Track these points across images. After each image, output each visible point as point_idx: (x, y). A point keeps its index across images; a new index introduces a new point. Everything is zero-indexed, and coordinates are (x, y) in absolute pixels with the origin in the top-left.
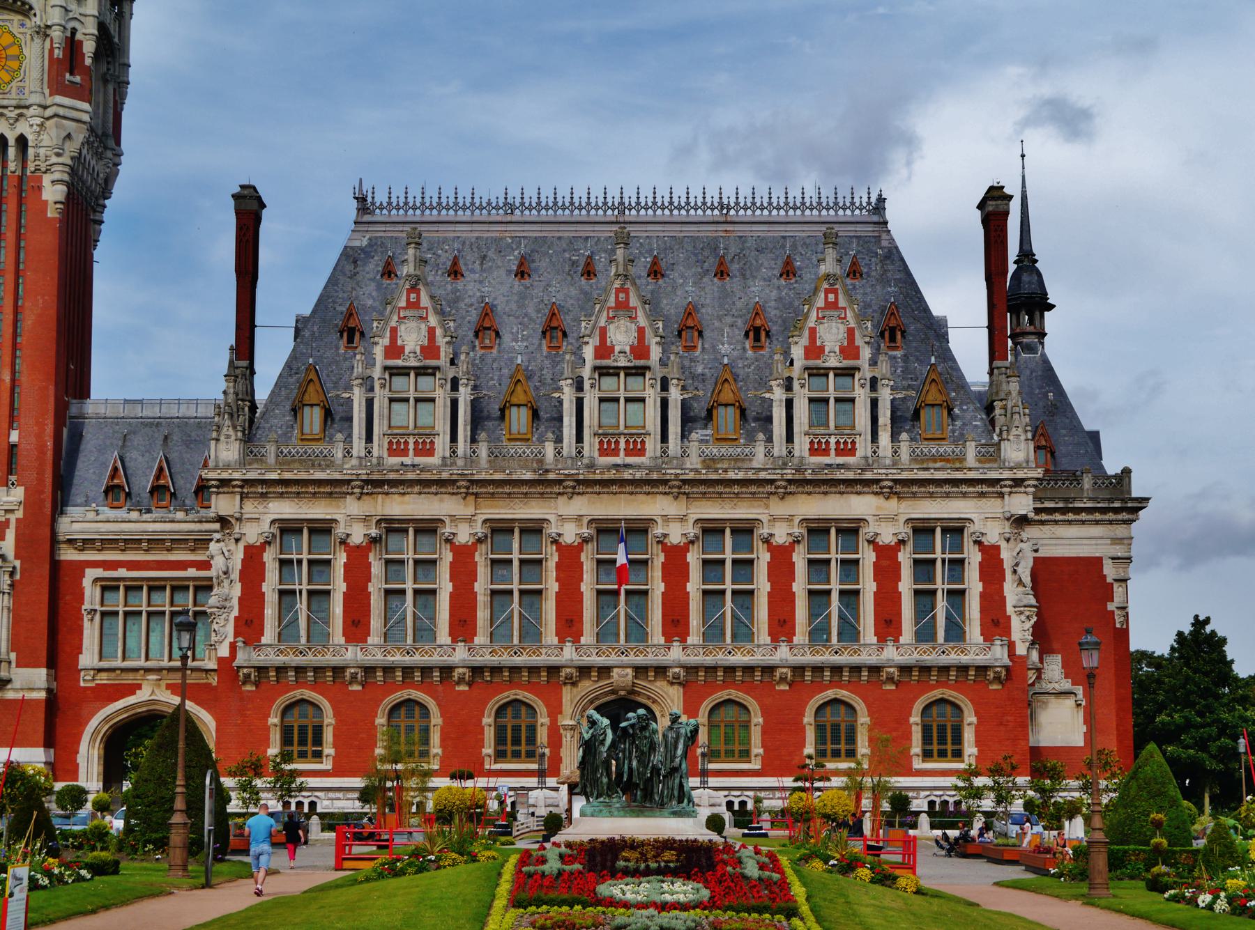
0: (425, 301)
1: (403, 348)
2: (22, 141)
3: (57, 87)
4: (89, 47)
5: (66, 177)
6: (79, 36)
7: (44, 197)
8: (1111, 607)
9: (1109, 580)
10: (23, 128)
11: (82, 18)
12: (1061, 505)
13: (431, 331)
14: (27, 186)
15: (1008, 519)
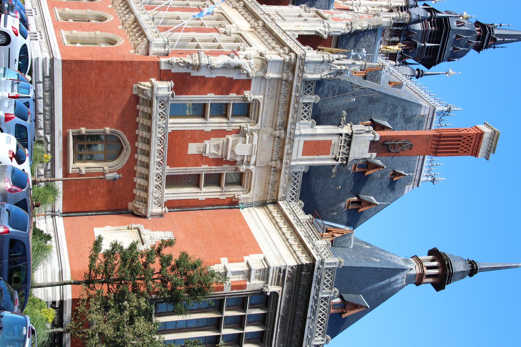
8: (224, 261)
9: (246, 258)
12: (293, 222)
15: (261, 55)
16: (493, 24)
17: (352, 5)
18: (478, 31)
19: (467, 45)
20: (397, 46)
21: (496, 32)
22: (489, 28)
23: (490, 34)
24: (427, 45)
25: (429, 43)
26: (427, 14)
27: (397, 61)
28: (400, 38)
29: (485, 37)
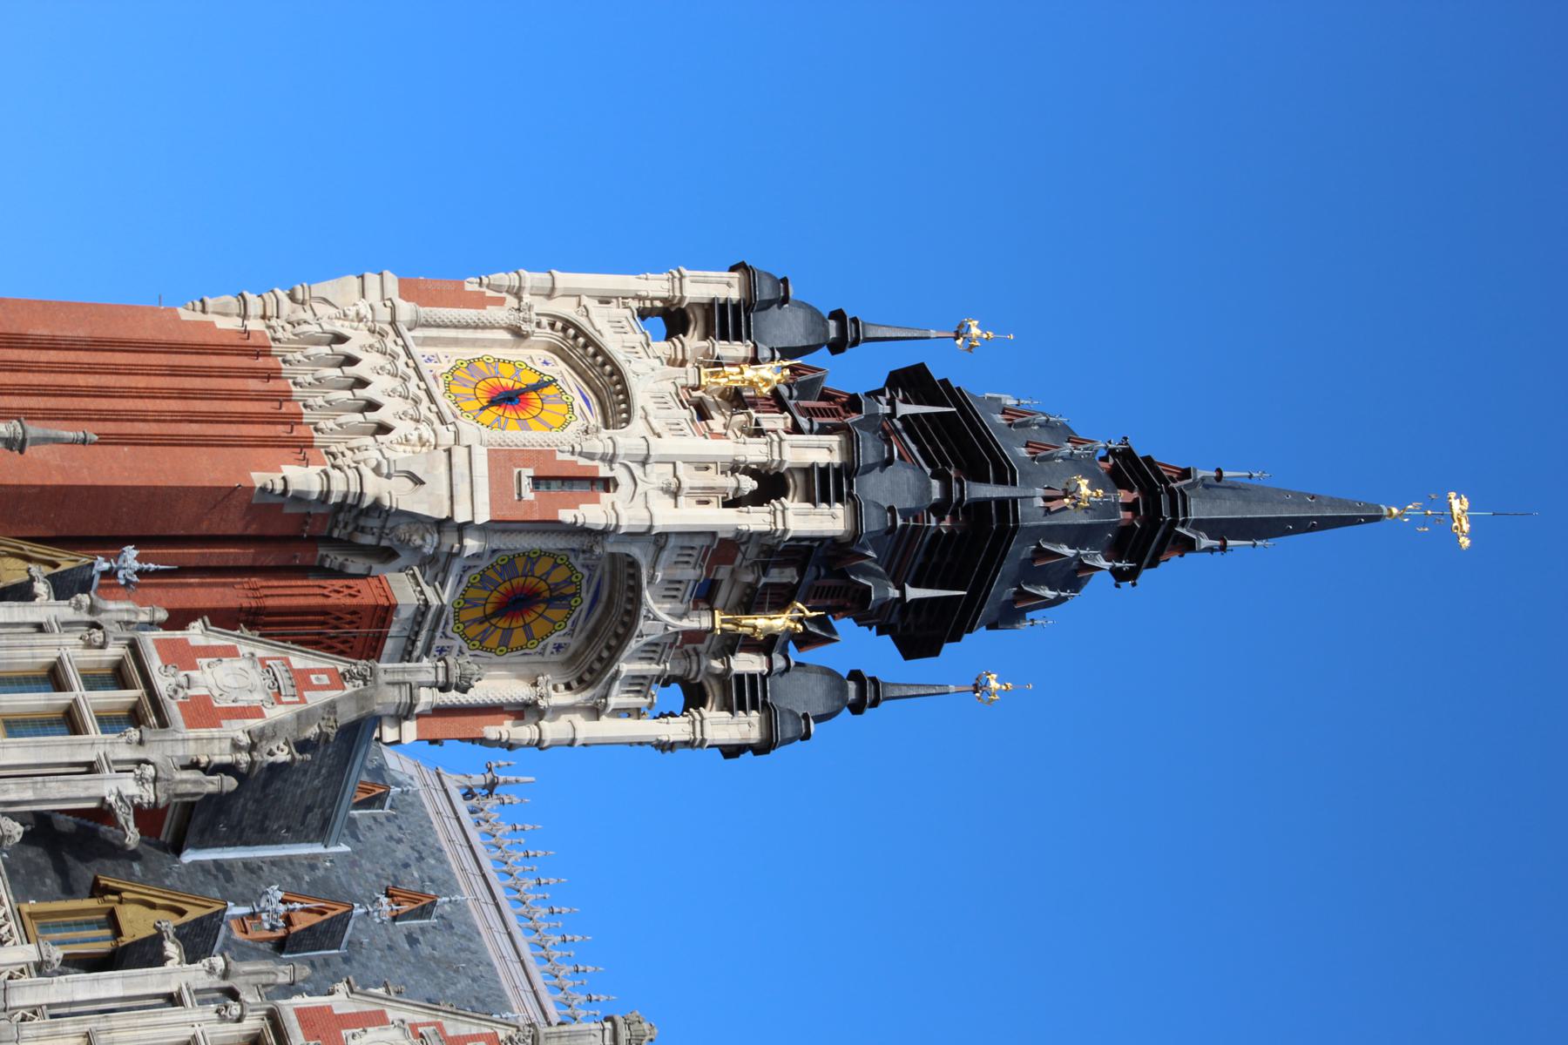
0: (315, 699)
1: (195, 667)
2: (383, 429)
3: (502, 459)
4: (592, 513)
5: (338, 486)
6: (605, 497)
7: (283, 467)
10: (402, 428)
11: (639, 499)
13: (257, 712)
14: (302, 448)
16: (1186, 473)
17: (610, 460)
18: (1126, 507)
19: (1073, 577)
20: (787, 614)
21: (1198, 509)
22: (1171, 492)
23: (1174, 523)
24: (913, 593)
25: (915, 585)
26: (929, 487)
27: (774, 655)
28: (801, 573)
29: (1150, 519)
